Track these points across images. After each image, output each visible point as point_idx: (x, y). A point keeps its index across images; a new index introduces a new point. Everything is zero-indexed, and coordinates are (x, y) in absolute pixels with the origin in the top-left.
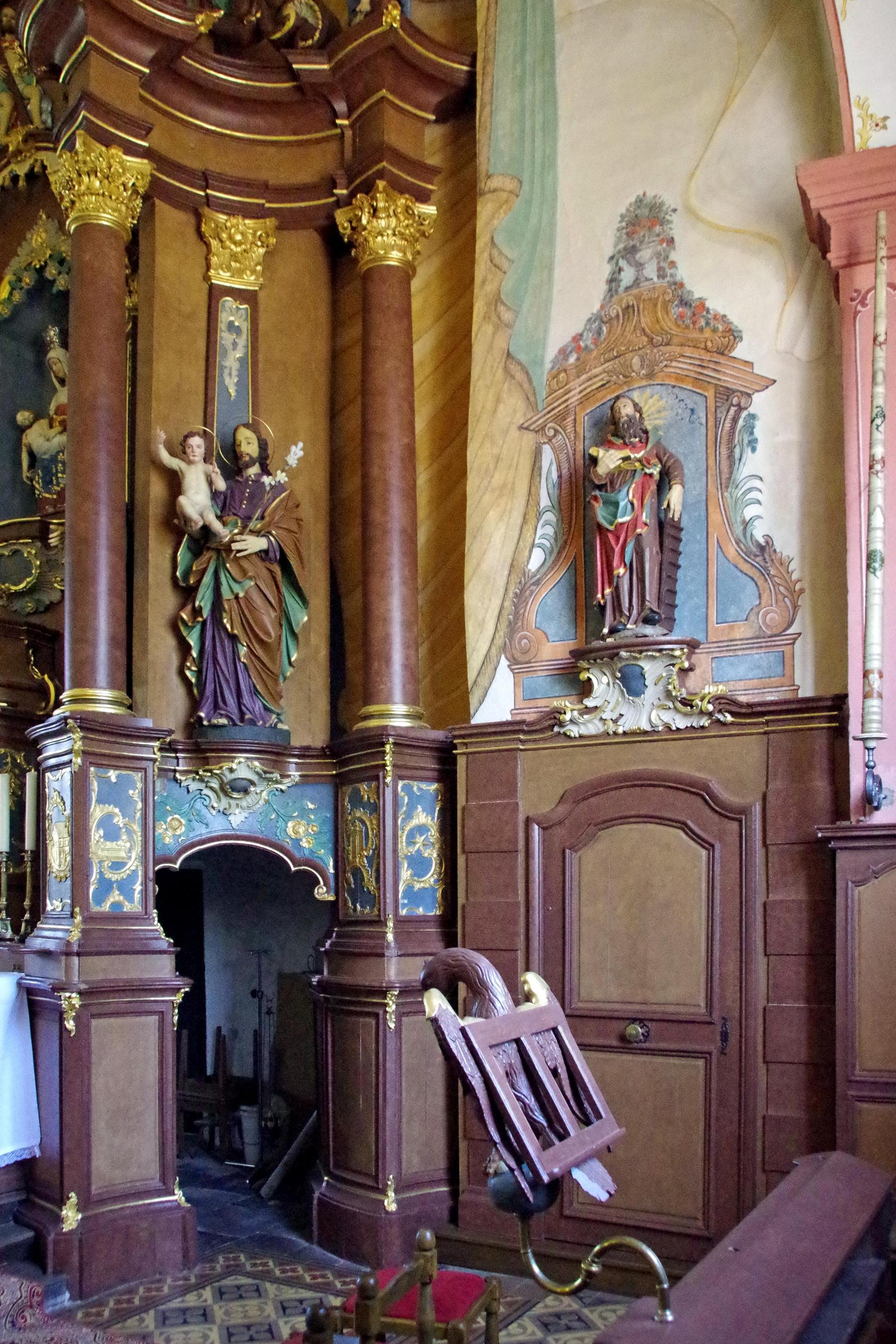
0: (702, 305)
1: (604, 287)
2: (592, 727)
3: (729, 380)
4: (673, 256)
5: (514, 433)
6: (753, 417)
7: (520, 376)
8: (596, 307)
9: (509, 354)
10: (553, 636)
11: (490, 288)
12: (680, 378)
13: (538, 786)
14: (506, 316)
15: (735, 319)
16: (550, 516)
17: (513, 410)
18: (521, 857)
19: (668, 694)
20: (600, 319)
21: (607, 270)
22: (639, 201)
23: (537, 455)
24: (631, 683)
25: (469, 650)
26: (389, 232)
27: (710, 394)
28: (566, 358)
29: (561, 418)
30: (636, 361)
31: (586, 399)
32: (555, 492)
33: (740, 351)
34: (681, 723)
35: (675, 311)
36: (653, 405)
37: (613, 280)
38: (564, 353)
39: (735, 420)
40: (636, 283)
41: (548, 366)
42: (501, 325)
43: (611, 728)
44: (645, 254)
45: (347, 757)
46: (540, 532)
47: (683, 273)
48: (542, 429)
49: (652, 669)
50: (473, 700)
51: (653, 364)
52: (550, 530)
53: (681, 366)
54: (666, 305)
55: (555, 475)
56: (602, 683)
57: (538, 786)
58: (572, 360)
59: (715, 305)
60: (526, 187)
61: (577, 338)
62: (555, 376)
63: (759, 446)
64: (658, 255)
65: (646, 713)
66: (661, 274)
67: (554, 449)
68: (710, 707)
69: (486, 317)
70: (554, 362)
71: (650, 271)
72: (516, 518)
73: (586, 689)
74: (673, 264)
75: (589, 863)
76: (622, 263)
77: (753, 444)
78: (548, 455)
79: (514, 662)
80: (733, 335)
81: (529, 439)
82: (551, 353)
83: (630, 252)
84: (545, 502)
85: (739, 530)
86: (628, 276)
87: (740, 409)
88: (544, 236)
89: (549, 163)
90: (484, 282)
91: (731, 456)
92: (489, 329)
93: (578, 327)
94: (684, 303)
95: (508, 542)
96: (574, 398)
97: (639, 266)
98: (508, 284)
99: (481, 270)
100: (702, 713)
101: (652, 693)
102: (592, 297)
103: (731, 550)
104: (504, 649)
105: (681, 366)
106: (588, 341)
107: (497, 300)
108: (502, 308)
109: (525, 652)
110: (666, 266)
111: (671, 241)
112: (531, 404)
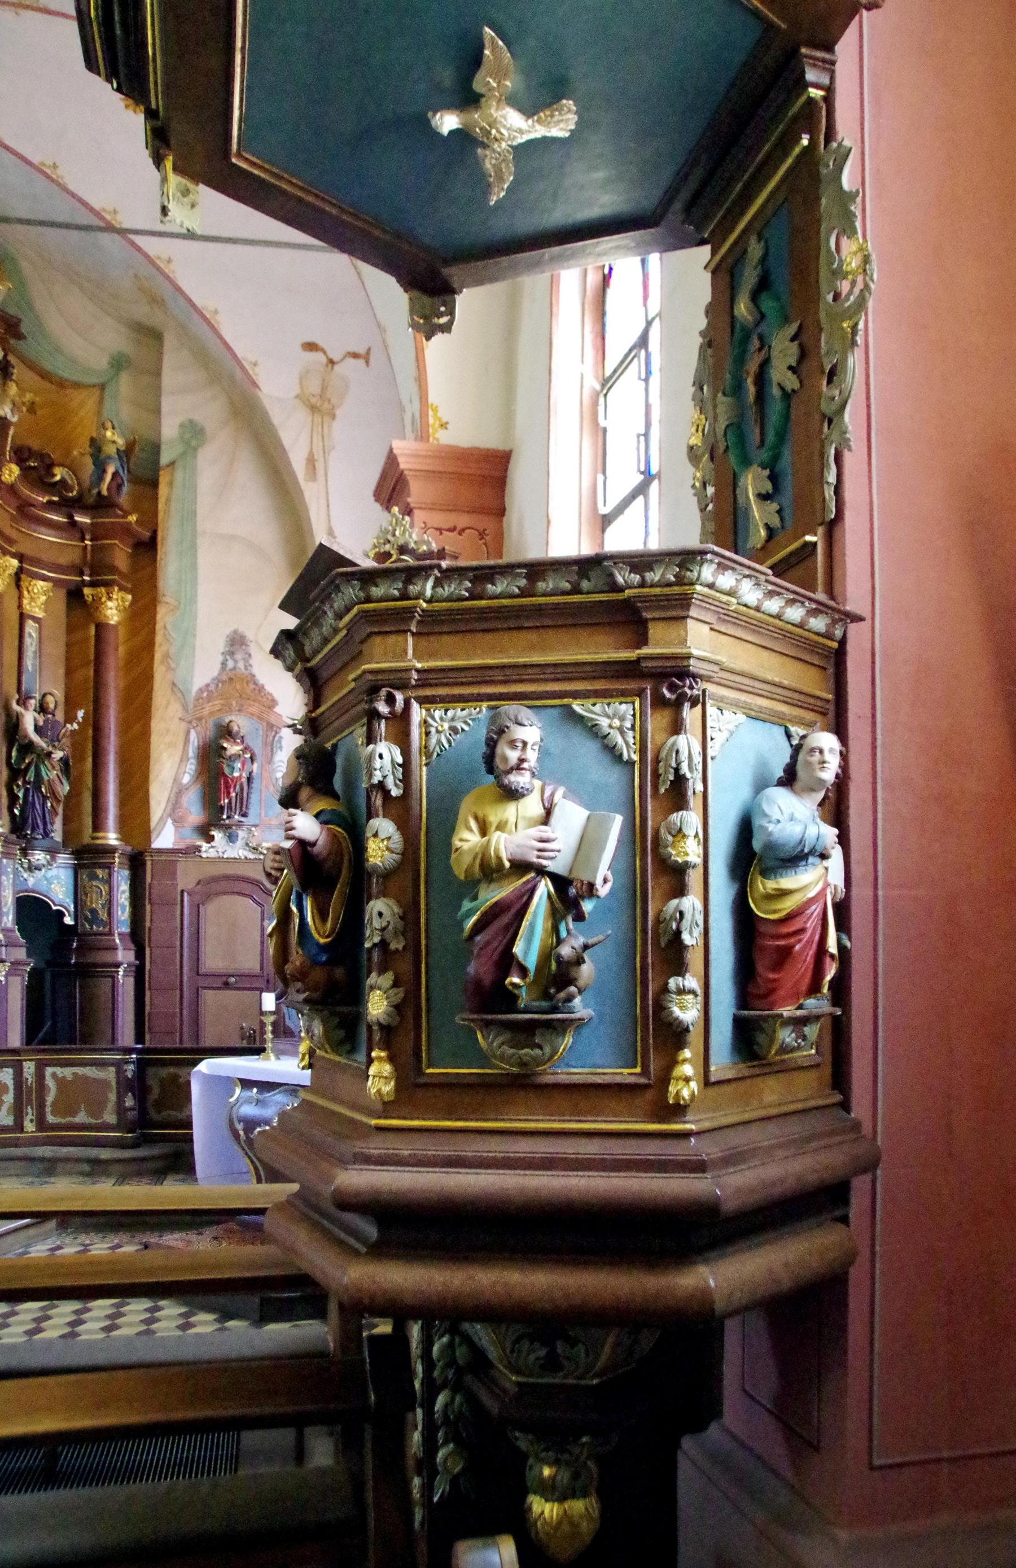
0: (263, 687)
1: (219, 666)
2: (212, 853)
3: (273, 720)
4: (251, 662)
5: (176, 720)
6: (281, 737)
7: (179, 695)
8: (216, 674)
9: (174, 684)
10: (195, 813)
11: (164, 648)
12: (252, 714)
13: (186, 877)
14: (173, 665)
15: (276, 696)
16: (193, 761)
17: (175, 709)
18: (179, 907)
19: (247, 844)
20: (217, 680)
21: (221, 658)
22: (235, 632)
23: (188, 733)
24: (232, 838)
25: (152, 815)
26: (113, 609)
27: (265, 724)
28: (203, 692)
29: (200, 719)
30: (234, 703)
31: (211, 713)
32: (196, 751)
33: (277, 709)
34: (251, 856)
35: (252, 686)
36: (240, 723)
37: (224, 664)
38: (201, 691)
39: (274, 737)
40: (234, 668)
41: (194, 694)
42: (169, 668)
43: (221, 854)
44: (239, 656)
45: (88, 859)
46: (188, 767)
47: (255, 670)
48: (190, 722)
49: (242, 834)
50: (153, 836)
51: (242, 705)
52: (193, 767)
53: (252, 709)
54: (247, 683)
55: (196, 744)
56: (218, 835)
57: (186, 877)
58: (205, 694)
59: (268, 688)
60: (182, 606)
61: (208, 685)
62: (198, 700)
63: (284, 750)
64: (244, 659)
65: (237, 851)
66: (246, 668)
67: (196, 732)
68: (265, 852)
69: (162, 662)
70: (197, 693)
71: (241, 665)
72: (177, 759)
73: (210, 839)
74: (251, 666)
75: (210, 911)
76: (228, 657)
77: (281, 748)
78: (193, 735)
79: (175, 821)
80: (273, 703)
81: (184, 725)
82: (195, 689)
83: (232, 654)
84: (191, 754)
85: (274, 781)
86: (230, 664)
87: (276, 733)
88: (190, 633)
89: (193, 599)
90: (161, 645)
91: (272, 751)
92: (164, 669)
93: (207, 680)
94: (255, 683)
95: (172, 771)
96: (206, 712)
97: (236, 661)
98: (173, 650)
99: (159, 639)
100: (261, 853)
101: (240, 843)
102: (215, 671)
103: (271, 788)
104: (170, 816)
105: (252, 709)
106: (212, 688)
107: (167, 656)
108: (170, 661)
109: (181, 818)
110: (248, 666)
111: (250, 655)
112: (185, 707)
